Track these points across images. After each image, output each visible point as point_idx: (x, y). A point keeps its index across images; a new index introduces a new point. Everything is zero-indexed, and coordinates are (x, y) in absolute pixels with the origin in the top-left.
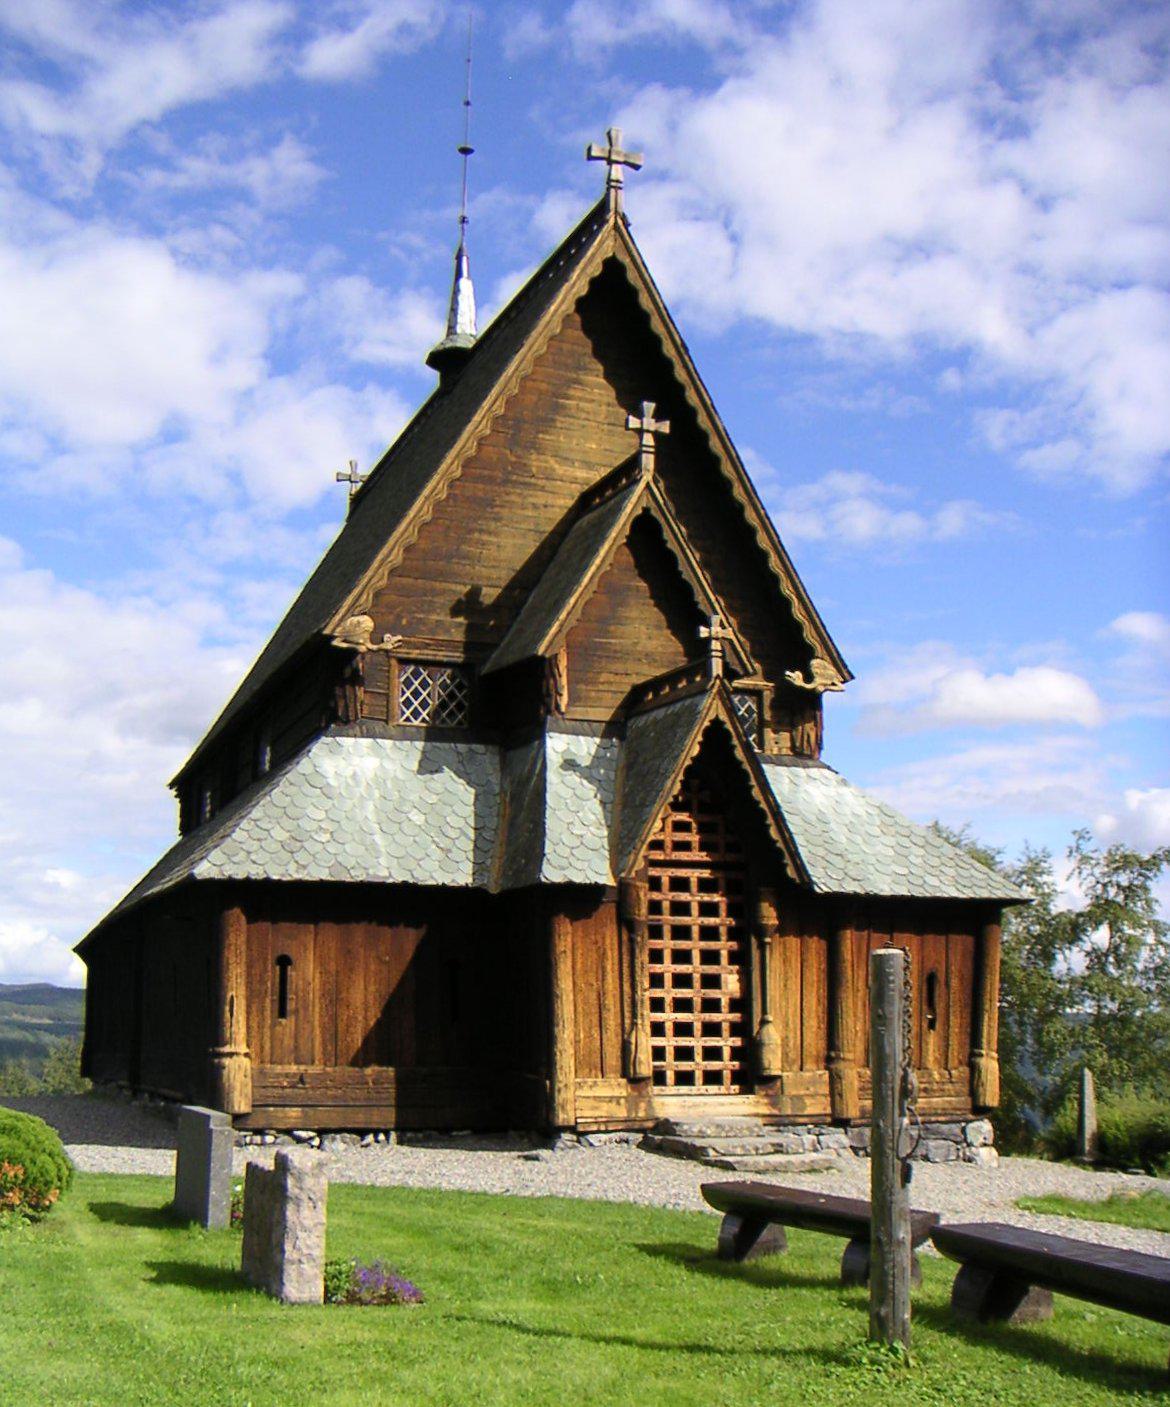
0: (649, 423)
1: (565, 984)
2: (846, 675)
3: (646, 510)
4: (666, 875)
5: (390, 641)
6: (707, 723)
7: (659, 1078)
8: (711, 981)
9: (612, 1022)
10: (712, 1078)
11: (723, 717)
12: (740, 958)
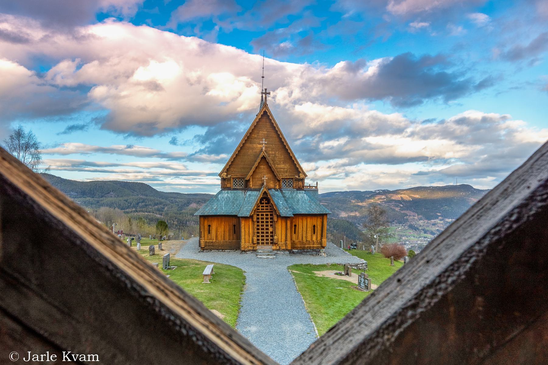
0: (264, 142)
1: (243, 230)
2: (306, 176)
4: (260, 214)
5: (229, 176)
7: (258, 243)
9: (251, 236)
10: (267, 243)
12: (271, 225)
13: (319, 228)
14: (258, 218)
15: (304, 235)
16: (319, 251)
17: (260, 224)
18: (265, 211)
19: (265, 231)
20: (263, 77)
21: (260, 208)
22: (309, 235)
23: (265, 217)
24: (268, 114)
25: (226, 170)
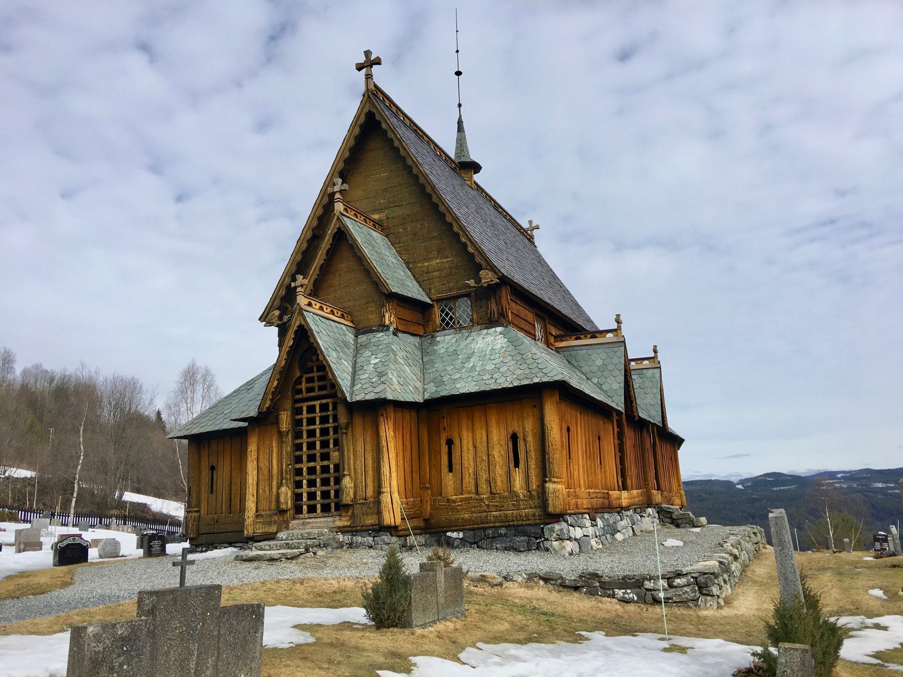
3: (339, 229)
6: (295, 328)
7: (298, 510)
8: (325, 457)
9: (275, 483)
10: (326, 509)
11: (303, 323)
14: (298, 423)
15: (484, 476)
17: (305, 439)
19: (318, 465)
20: (458, 73)
21: (304, 386)
22: (499, 471)
23: (318, 414)
24: (377, 117)
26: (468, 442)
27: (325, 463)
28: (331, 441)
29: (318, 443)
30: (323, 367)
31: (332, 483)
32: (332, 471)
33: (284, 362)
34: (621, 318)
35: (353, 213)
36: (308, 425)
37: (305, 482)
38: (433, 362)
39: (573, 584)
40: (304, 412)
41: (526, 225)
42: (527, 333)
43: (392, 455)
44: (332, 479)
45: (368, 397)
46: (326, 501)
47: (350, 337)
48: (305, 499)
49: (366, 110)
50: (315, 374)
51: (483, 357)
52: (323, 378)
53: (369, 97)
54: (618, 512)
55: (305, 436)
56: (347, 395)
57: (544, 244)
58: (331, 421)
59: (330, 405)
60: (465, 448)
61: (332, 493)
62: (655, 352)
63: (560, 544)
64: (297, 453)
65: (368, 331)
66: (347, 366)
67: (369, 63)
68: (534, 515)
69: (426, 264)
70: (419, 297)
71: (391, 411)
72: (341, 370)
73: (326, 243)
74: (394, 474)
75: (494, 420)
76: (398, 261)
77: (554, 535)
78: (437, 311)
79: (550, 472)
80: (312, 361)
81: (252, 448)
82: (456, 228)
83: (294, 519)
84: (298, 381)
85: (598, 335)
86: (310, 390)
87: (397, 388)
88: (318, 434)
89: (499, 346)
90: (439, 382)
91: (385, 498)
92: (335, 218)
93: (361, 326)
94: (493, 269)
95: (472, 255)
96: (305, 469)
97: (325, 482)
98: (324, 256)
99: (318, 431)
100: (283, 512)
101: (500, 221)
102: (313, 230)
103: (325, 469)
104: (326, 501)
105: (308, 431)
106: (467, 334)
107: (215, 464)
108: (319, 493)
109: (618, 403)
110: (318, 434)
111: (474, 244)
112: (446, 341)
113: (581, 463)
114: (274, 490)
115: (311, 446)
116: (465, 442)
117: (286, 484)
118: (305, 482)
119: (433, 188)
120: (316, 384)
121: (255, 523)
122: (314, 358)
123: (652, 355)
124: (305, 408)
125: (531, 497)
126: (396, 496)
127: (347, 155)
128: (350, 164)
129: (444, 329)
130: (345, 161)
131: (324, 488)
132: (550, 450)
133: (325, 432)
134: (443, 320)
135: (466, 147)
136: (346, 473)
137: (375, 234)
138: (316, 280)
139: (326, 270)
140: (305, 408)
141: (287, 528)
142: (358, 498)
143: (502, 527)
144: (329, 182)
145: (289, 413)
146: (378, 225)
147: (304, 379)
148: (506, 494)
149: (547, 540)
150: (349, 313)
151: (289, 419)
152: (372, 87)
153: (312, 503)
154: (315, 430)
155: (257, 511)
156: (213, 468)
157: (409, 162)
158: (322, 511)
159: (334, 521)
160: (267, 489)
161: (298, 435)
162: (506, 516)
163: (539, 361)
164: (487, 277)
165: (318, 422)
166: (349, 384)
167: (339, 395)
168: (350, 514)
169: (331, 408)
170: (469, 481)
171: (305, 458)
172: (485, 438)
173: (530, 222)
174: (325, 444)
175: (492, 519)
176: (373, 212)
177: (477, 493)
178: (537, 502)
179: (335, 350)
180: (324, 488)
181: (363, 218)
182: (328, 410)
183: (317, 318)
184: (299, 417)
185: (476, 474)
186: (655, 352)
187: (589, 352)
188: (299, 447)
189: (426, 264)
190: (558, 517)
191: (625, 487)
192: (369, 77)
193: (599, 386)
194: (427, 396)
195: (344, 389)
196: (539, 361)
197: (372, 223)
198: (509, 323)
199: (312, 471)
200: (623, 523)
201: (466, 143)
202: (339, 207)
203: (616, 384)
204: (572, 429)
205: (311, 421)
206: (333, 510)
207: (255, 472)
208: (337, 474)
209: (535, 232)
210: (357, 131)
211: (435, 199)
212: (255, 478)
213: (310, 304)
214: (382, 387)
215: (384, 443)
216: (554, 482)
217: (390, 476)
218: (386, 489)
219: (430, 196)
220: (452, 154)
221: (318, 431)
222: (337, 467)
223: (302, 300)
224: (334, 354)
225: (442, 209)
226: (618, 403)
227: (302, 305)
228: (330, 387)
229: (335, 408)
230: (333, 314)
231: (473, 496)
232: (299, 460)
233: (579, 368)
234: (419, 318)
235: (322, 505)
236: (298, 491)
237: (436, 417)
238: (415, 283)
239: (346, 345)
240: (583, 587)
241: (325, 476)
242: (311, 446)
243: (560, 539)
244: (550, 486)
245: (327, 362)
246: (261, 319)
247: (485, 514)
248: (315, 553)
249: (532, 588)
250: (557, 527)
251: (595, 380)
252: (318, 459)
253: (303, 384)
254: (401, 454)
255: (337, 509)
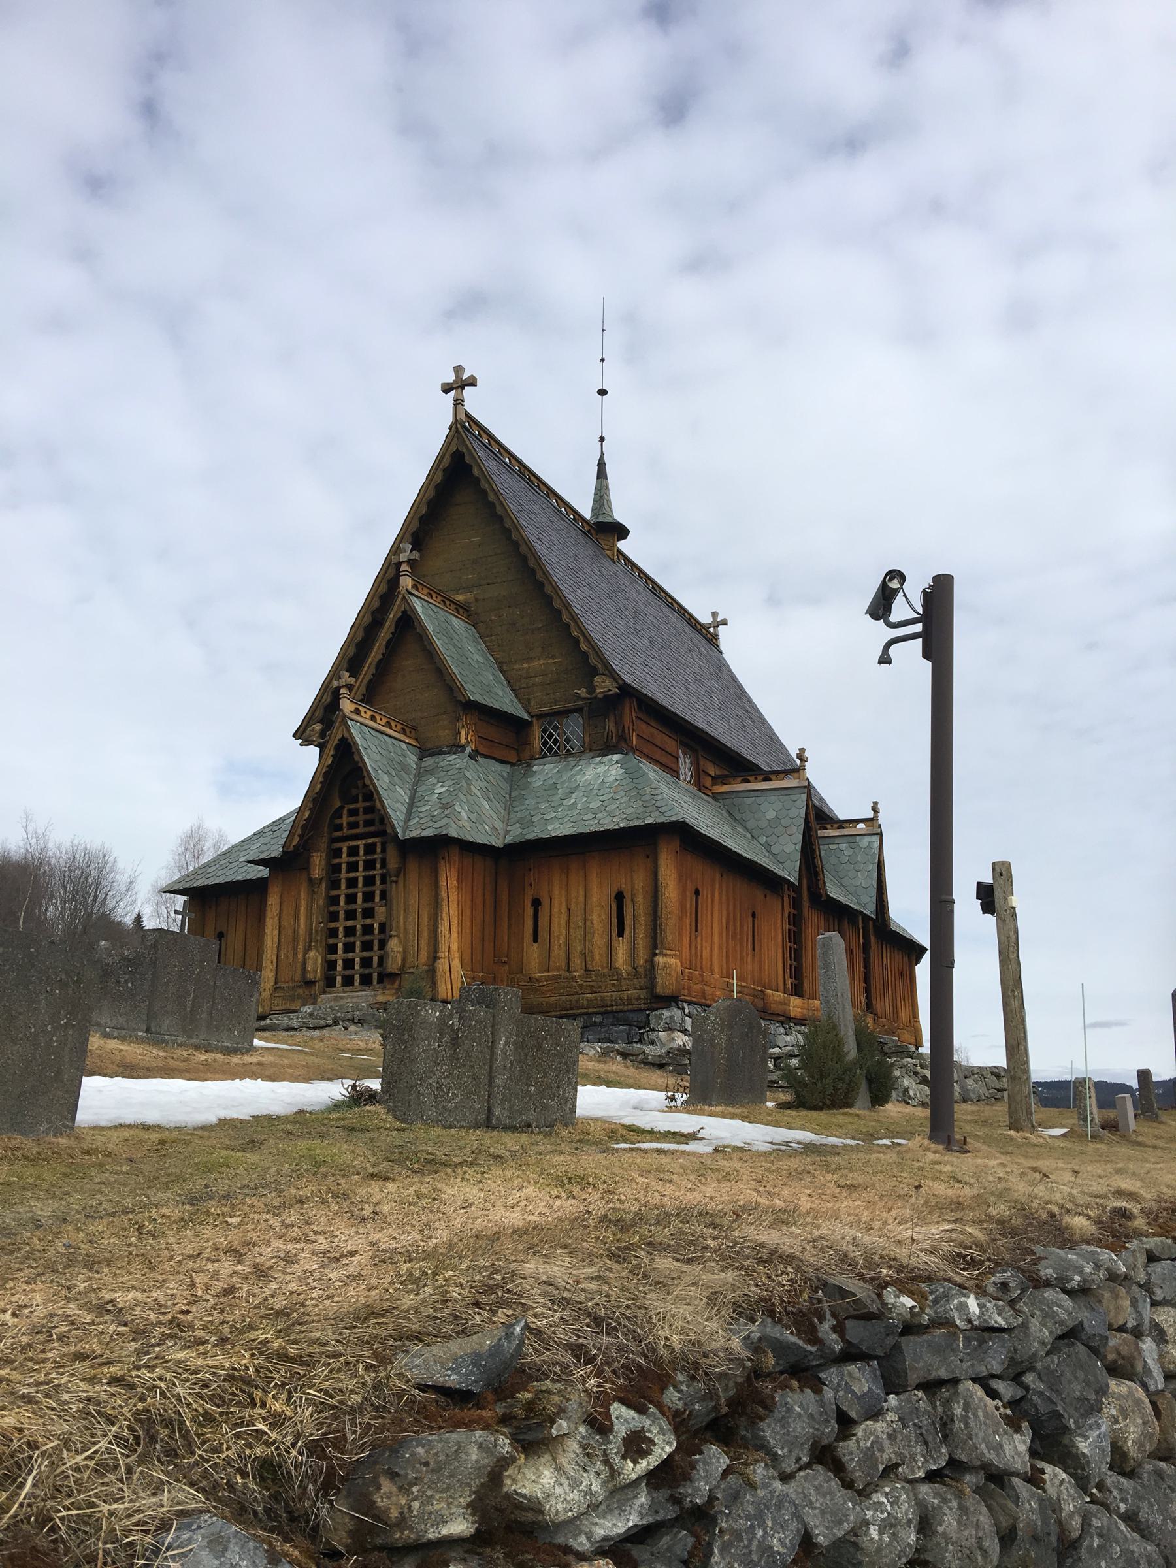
3: (404, 612)
6: (336, 742)
7: (330, 982)
8: (369, 913)
9: (301, 947)
10: (366, 981)
13: (637, 909)
16: (645, 1025)
18: (361, 830)
20: (602, 392)
21: (345, 820)
22: (598, 940)
23: (362, 857)
24: (468, 459)
25: (319, 713)
26: (560, 904)
27: (368, 921)
28: (377, 893)
29: (360, 895)
30: (371, 795)
31: (376, 948)
32: (376, 932)
33: (319, 786)
34: (806, 754)
35: (426, 591)
36: (348, 871)
37: (340, 946)
38: (522, 797)
39: (657, 1061)
40: (344, 855)
41: (705, 618)
42: (665, 767)
43: (454, 912)
44: (376, 943)
45: (425, 834)
46: (367, 971)
47: (412, 759)
48: (339, 968)
49: (453, 448)
50: (360, 805)
51: (589, 792)
52: (371, 810)
53: (457, 431)
54: (782, 1023)
55: (343, 886)
56: (399, 830)
57: (738, 650)
58: (378, 866)
59: (379, 845)
60: (555, 910)
61: (375, 959)
62: (875, 809)
63: (669, 1035)
64: (333, 909)
65: (437, 752)
66: (403, 794)
67: (459, 384)
68: (639, 998)
69: (525, 666)
70: (511, 710)
71: (455, 852)
72: (395, 800)
73: (385, 633)
74: (455, 935)
75: (595, 875)
76: (487, 659)
77: (662, 1024)
78: (537, 733)
79: (662, 942)
80: (357, 788)
81: (273, 900)
82: (565, 618)
83: (324, 992)
84: (338, 814)
85: (773, 777)
86: (353, 825)
87: (466, 824)
88: (360, 884)
89: (612, 778)
90: (526, 823)
91: (442, 965)
92: (400, 597)
93: (429, 746)
94: (612, 674)
95: (585, 655)
96: (341, 929)
97: (367, 946)
98: (383, 650)
99: (360, 880)
100: (310, 983)
101: (653, 610)
102: (373, 613)
103: (368, 929)
104: (367, 971)
105: (348, 880)
106: (573, 763)
107: (224, 931)
108: (357, 960)
109: (790, 871)
110: (360, 884)
111: (588, 639)
112: (545, 771)
113: (716, 939)
114: (300, 956)
115: (351, 899)
116: (556, 902)
117: (316, 947)
118: (340, 946)
119: (538, 559)
120: (361, 818)
121: (273, 997)
122: (360, 783)
123: (870, 815)
124: (345, 850)
125: (636, 975)
126: (456, 963)
127: (424, 510)
128: (426, 524)
129: (545, 756)
130: (421, 518)
131: (366, 954)
132: (663, 913)
133: (369, 881)
134: (545, 743)
135: (609, 500)
136: (393, 933)
137: (456, 622)
138: (371, 681)
139: (384, 668)
140: (345, 850)
141: (314, 1003)
142: (407, 965)
143: (597, 1013)
144: (395, 549)
145: (324, 855)
146: (462, 610)
147: (345, 812)
148: (606, 970)
149: (653, 1030)
150: (414, 728)
151: (323, 863)
152: (462, 416)
153: (348, 972)
154: (356, 879)
155: (276, 983)
156: (220, 936)
157: (508, 524)
158: (361, 983)
159: (375, 995)
160: (290, 954)
161: (335, 885)
162: (603, 999)
163: (658, 798)
164: (603, 685)
165: (361, 869)
166: (403, 817)
167: (389, 831)
168: (396, 986)
169: (379, 850)
170: (558, 953)
171: (342, 915)
172: (582, 899)
173: (714, 614)
174: (368, 897)
175: (585, 1003)
176: (457, 591)
177: (568, 970)
178: (643, 981)
179: (388, 773)
180: (366, 954)
181: (440, 598)
182: (375, 852)
183: (366, 730)
184: (337, 861)
185: (568, 945)
186: (875, 809)
187: (759, 800)
188: (334, 901)
189: (525, 666)
190: (671, 1000)
191: (798, 991)
192: (458, 402)
193: (768, 847)
194: (508, 839)
195: (395, 822)
196: (658, 798)
197: (453, 606)
198: (634, 750)
199: (350, 931)
200: (788, 1038)
201: (608, 495)
202: (406, 582)
203: (791, 844)
204: (704, 892)
205: (352, 867)
206: (375, 982)
207: (276, 932)
208: (382, 936)
209: (721, 629)
210: (439, 477)
211: (539, 575)
212: (276, 940)
213: (357, 711)
214: (446, 820)
215: (444, 895)
216: (666, 955)
217: (450, 937)
218: (443, 954)
219: (533, 571)
220: (586, 510)
221: (360, 880)
222: (383, 927)
223: (347, 706)
224: (386, 778)
225: (548, 589)
226: (790, 871)
227: (346, 711)
228: (378, 820)
229: (384, 850)
230: (391, 728)
231: (563, 973)
232: (334, 917)
233: (742, 823)
234: (511, 740)
235: (361, 976)
236: (332, 957)
237: (517, 867)
238: (508, 690)
239: (404, 767)
240: (669, 1064)
241: (367, 938)
242: (351, 899)
243: (669, 1029)
244: (660, 960)
245: (375, 786)
246: (296, 735)
247: (576, 997)
248: (346, 1029)
249: (605, 1062)
250: (666, 1013)
251: (763, 839)
252: (359, 915)
253: (345, 817)
254: (469, 913)
255: (380, 981)
